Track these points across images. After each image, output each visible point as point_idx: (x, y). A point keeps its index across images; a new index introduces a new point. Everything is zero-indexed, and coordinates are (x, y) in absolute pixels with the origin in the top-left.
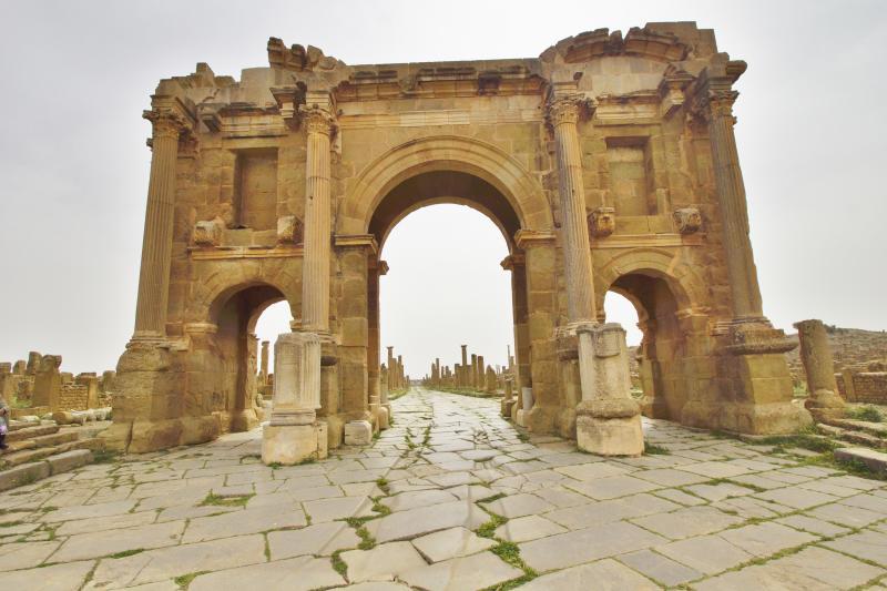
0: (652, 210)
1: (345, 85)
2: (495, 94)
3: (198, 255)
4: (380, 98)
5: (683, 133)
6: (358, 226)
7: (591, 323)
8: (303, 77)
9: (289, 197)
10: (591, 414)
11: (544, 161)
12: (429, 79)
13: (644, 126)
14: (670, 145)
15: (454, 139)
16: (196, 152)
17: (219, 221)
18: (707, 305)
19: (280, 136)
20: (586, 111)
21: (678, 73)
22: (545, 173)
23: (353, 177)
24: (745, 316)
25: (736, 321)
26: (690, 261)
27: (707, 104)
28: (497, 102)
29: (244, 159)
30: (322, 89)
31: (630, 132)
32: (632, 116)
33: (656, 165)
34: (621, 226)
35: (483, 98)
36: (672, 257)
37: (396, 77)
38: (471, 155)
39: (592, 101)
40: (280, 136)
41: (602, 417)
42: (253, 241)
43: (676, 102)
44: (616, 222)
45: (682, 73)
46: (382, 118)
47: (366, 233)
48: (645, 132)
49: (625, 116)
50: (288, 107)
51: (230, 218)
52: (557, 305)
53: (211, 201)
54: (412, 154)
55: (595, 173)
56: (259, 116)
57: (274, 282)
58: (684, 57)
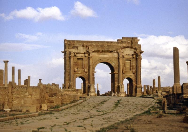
1: (93, 51)
7: (121, 84)
12: (104, 51)
28: (112, 53)
31: (129, 59)
32: (129, 57)
33: (131, 64)
36: (132, 76)
43: (134, 57)
48: (130, 59)
58: (136, 50)
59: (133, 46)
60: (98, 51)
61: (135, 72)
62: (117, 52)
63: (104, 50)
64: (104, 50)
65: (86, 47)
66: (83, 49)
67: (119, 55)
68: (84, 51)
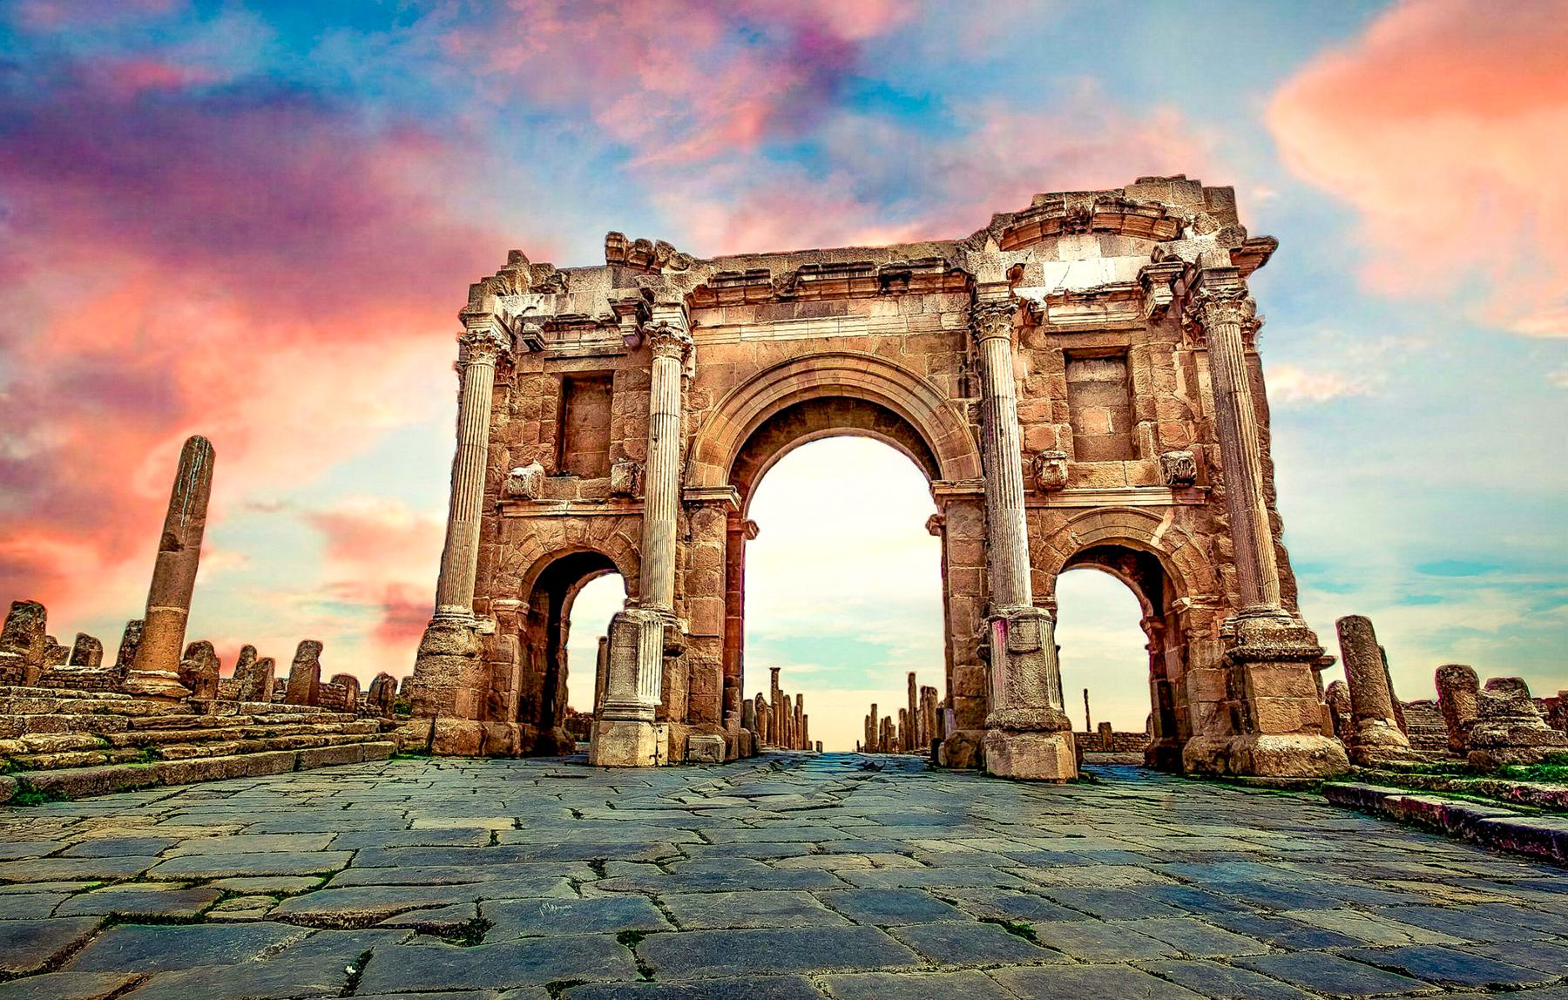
0: (1134, 453)
1: (702, 290)
2: (904, 292)
3: (511, 512)
4: (748, 302)
5: (1181, 340)
6: (714, 476)
8: (646, 280)
9: (624, 436)
10: (1001, 726)
11: (971, 383)
13: (1120, 332)
14: (1156, 358)
15: (845, 356)
16: (513, 379)
17: (537, 467)
18: (1212, 592)
19: (616, 356)
20: (1033, 317)
21: (1166, 259)
22: (973, 401)
23: (709, 409)
24: (1252, 607)
25: (1245, 615)
26: (1187, 526)
27: (1201, 306)
28: (907, 302)
29: (571, 386)
30: (672, 300)
31: (1100, 341)
32: (1102, 318)
33: (1137, 389)
34: (1076, 476)
35: (887, 298)
36: (1160, 521)
37: (769, 277)
38: (870, 378)
39: (1036, 304)
40: (616, 356)
41: (1011, 730)
42: (578, 493)
44: (1071, 469)
45: (1173, 258)
46: (748, 329)
47: (723, 484)
48: (1124, 341)
49: (1091, 319)
50: (628, 321)
51: (551, 463)
52: (985, 587)
53: (528, 441)
54: (790, 376)
55: (1047, 400)
56: (590, 330)
57: (604, 548)
58: (1180, 235)
59: (1140, 202)
60: (757, 288)
61: (1194, 465)
63: (809, 270)
64: (809, 270)
66: (616, 286)
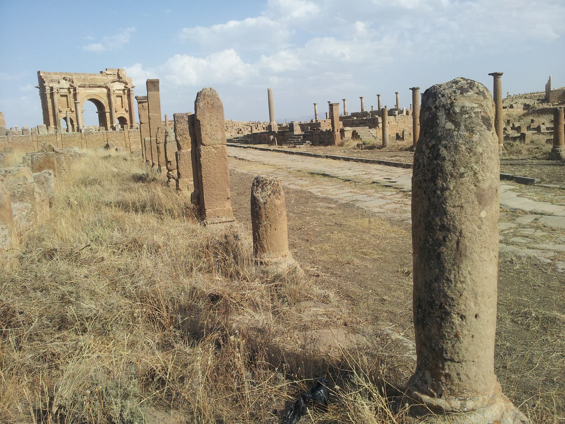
29: (62, 96)
45: (127, 88)
48: (121, 95)
58: (127, 84)
62: (106, 87)
63: (91, 85)
65: (70, 81)
66: (66, 83)
67: (109, 90)
68: (68, 86)
